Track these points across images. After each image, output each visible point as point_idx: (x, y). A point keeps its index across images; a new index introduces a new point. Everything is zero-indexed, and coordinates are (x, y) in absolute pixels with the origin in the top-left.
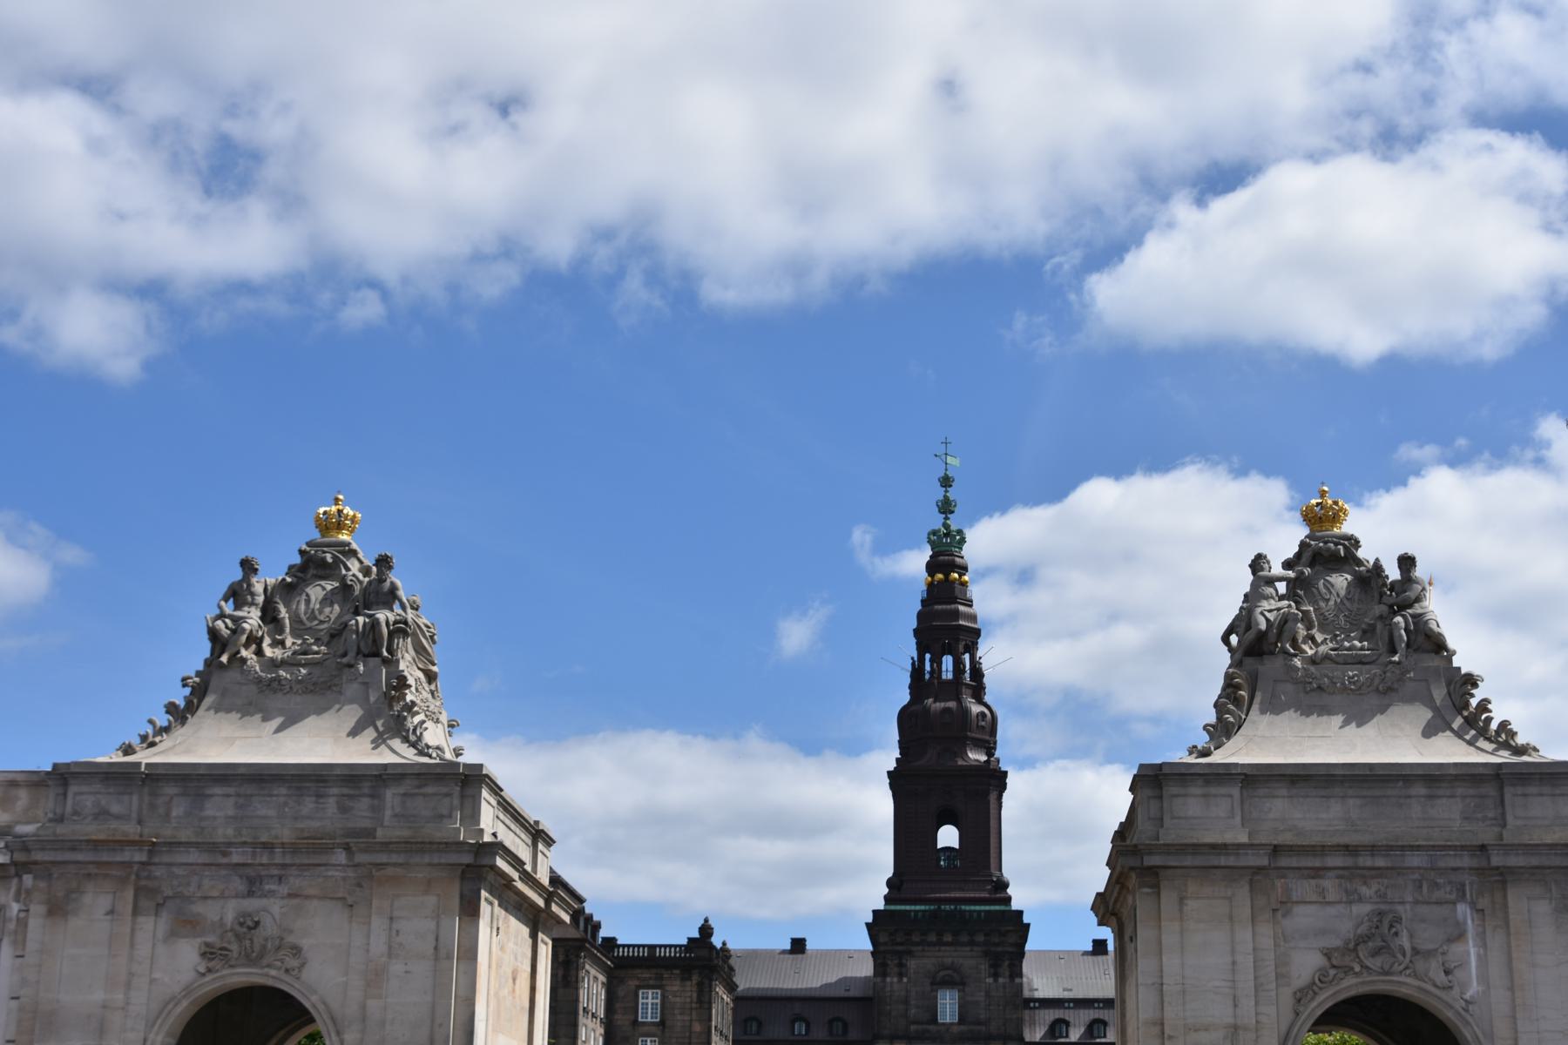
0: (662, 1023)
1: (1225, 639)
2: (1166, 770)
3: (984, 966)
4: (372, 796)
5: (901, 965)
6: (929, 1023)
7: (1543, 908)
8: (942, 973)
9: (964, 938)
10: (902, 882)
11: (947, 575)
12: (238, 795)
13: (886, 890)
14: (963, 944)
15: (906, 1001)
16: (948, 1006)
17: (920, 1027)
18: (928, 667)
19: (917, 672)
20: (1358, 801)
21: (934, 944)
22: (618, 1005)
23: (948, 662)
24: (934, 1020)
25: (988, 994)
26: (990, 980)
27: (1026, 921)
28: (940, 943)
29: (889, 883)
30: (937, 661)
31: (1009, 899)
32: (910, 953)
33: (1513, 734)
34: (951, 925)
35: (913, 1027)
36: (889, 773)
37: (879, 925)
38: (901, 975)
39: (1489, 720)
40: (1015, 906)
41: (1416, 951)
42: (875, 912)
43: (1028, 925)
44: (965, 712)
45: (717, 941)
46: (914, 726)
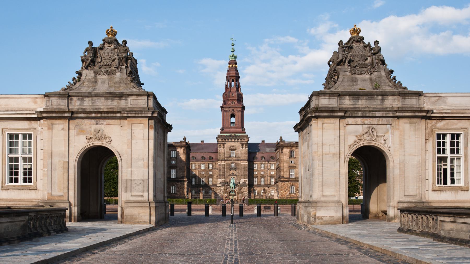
0: (176, 158)
1: (329, 64)
2: (320, 93)
3: (240, 146)
4: (126, 100)
7: (407, 126)
12: (92, 100)
18: (229, 85)
19: (227, 86)
20: (365, 100)
23: (233, 84)
24: (230, 157)
25: (241, 152)
30: (231, 84)
31: (245, 133)
33: (401, 84)
37: (219, 137)
39: (395, 81)
40: (246, 134)
41: (377, 136)
45: (187, 141)
46: (226, 98)
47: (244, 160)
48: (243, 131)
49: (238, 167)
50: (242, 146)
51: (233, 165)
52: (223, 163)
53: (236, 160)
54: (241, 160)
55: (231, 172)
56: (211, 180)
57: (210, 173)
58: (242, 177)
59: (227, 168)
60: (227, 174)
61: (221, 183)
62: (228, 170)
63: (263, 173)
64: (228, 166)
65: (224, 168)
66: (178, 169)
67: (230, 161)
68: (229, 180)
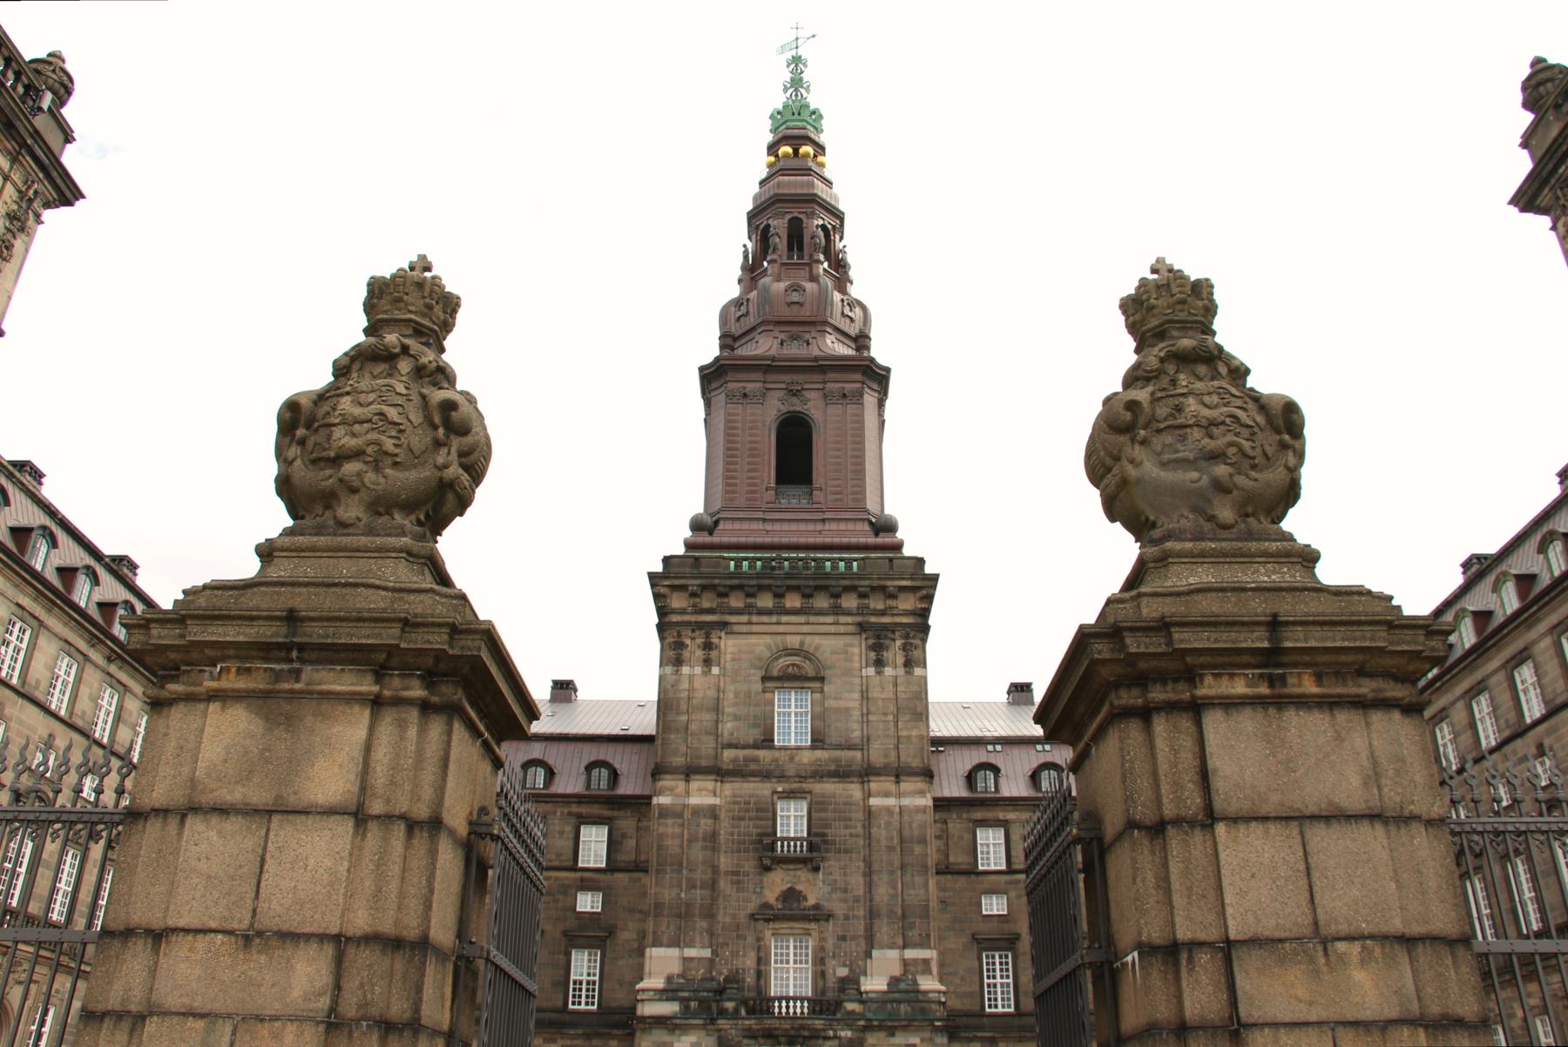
3: (857, 648)
5: (708, 646)
6: (756, 746)
8: (783, 661)
9: (822, 602)
10: (716, 523)
11: (796, 152)
13: (688, 534)
14: (821, 613)
15: (717, 708)
16: (792, 721)
17: (741, 753)
21: (769, 612)
24: (767, 742)
25: (865, 696)
26: (871, 671)
27: (928, 570)
29: (697, 525)
31: (898, 547)
34: (796, 582)
35: (728, 754)
36: (702, 369)
38: (707, 662)
43: (934, 578)
48: (883, 539)
49: (837, 832)
50: (878, 648)
51: (792, 821)
52: (702, 794)
53: (819, 774)
54: (866, 773)
55: (777, 882)
56: (583, 966)
57: (587, 903)
58: (884, 929)
60: (736, 904)
61: (667, 993)
62: (749, 865)
64: (750, 828)
65: (712, 837)
67: (765, 775)
68: (750, 962)
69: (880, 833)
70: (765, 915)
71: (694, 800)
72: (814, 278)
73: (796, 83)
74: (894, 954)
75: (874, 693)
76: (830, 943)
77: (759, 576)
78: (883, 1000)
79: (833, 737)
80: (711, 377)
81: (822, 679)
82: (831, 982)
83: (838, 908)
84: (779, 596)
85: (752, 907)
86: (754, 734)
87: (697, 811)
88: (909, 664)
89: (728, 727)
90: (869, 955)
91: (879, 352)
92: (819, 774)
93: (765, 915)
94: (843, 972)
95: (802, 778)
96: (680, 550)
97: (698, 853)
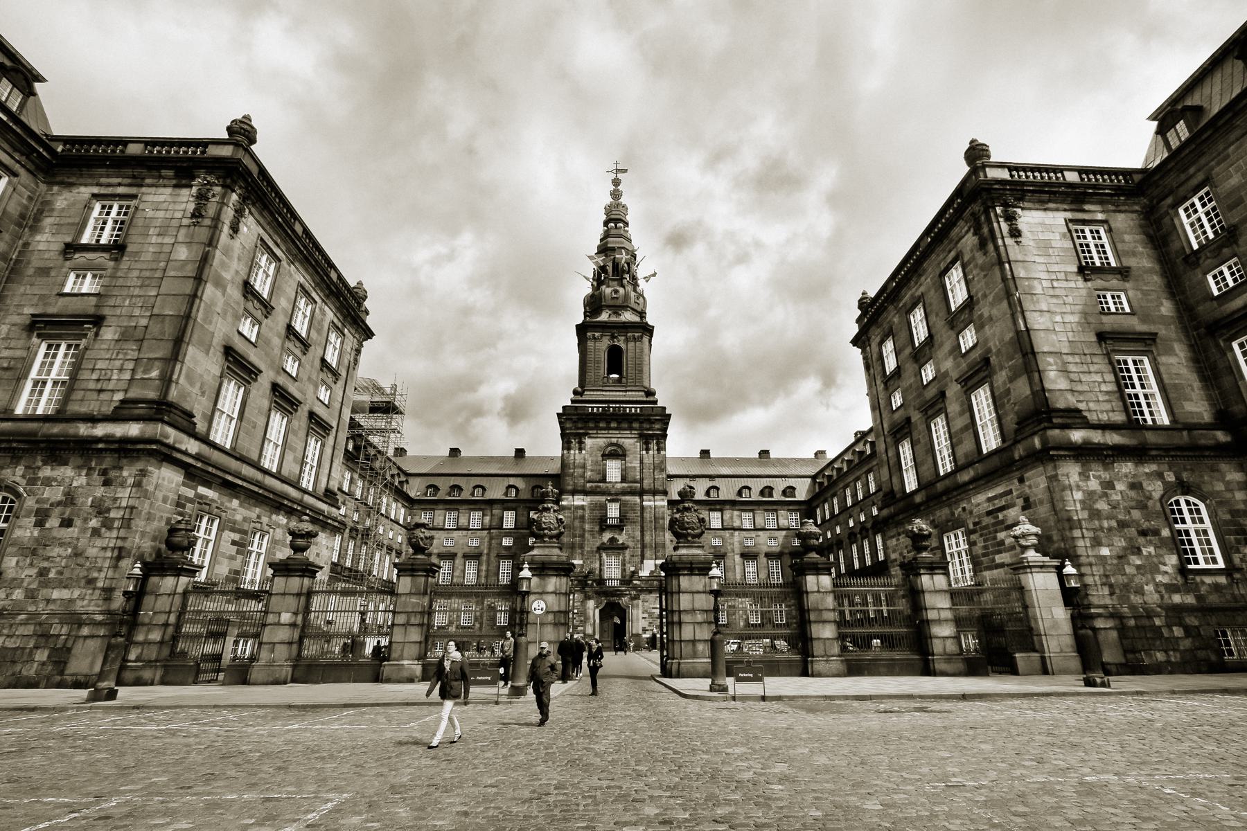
0: (117, 249)
5: (581, 443)
6: (600, 482)
9: (625, 425)
15: (584, 467)
16: (613, 470)
22: (48, 221)
24: (604, 480)
25: (641, 462)
28: (609, 428)
29: (575, 392)
31: (655, 402)
32: (586, 434)
34: (614, 418)
35: (589, 485)
38: (580, 449)
40: (659, 404)
42: (564, 408)
44: (627, 296)
47: (654, 492)
48: (651, 399)
49: (631, 515)
50: (647, 443)
51: (613, 511)
52: (579, 501)
53: (624, 493)
54: (641, 493)
55: (607, 536)
58: (648, 553)
59: (592, 521)
62: (597, 528)
63: (717, 542)
64: (597, 513)
65: (583, 517)
66: (108, 334)
67: (603, 493)
68: (597, 565)
69: (647, 515)
70: (602, 548)
71: (576, 503)
72: (623, 286)
73: (616, 195)
74: (652, 562)
75: (645, 461)
76: (627, 558)
77: (600, 414)
78: (647, 580)
79: (629, 478)
80: (581, 330)
81: (625, 455)
82: (628, 573)
83: (631, 544)
84: (608, 423)
85: (598, 544)
86: (598, 477)
87: (578, 507)
88: (659, 450)
89: (588, 474)
90: (642, 562)
91: (650, 320)
92: (624, 493)
93: (602, 548)
94: (632, 569)
95: (617, 494)
96: (569, 403)
97: (577, 523)
